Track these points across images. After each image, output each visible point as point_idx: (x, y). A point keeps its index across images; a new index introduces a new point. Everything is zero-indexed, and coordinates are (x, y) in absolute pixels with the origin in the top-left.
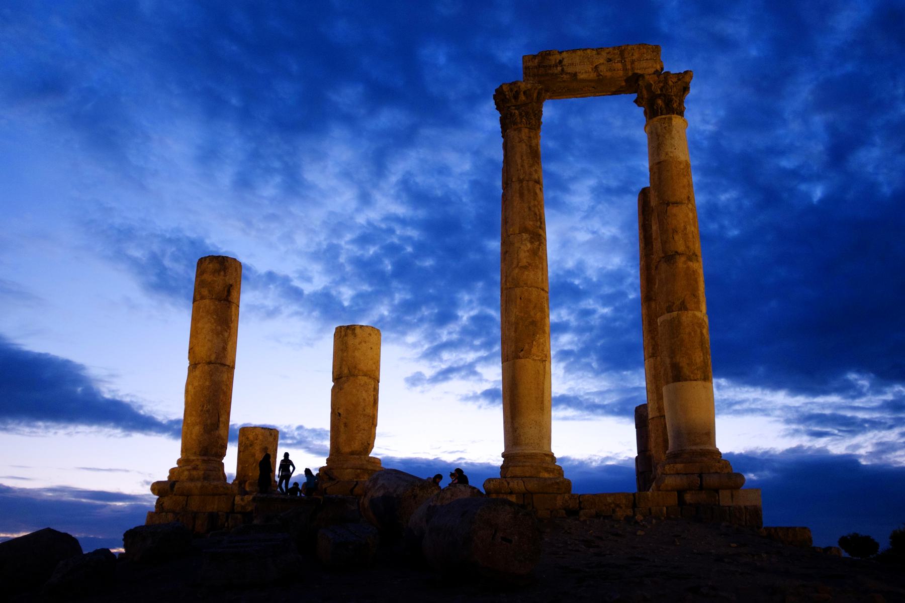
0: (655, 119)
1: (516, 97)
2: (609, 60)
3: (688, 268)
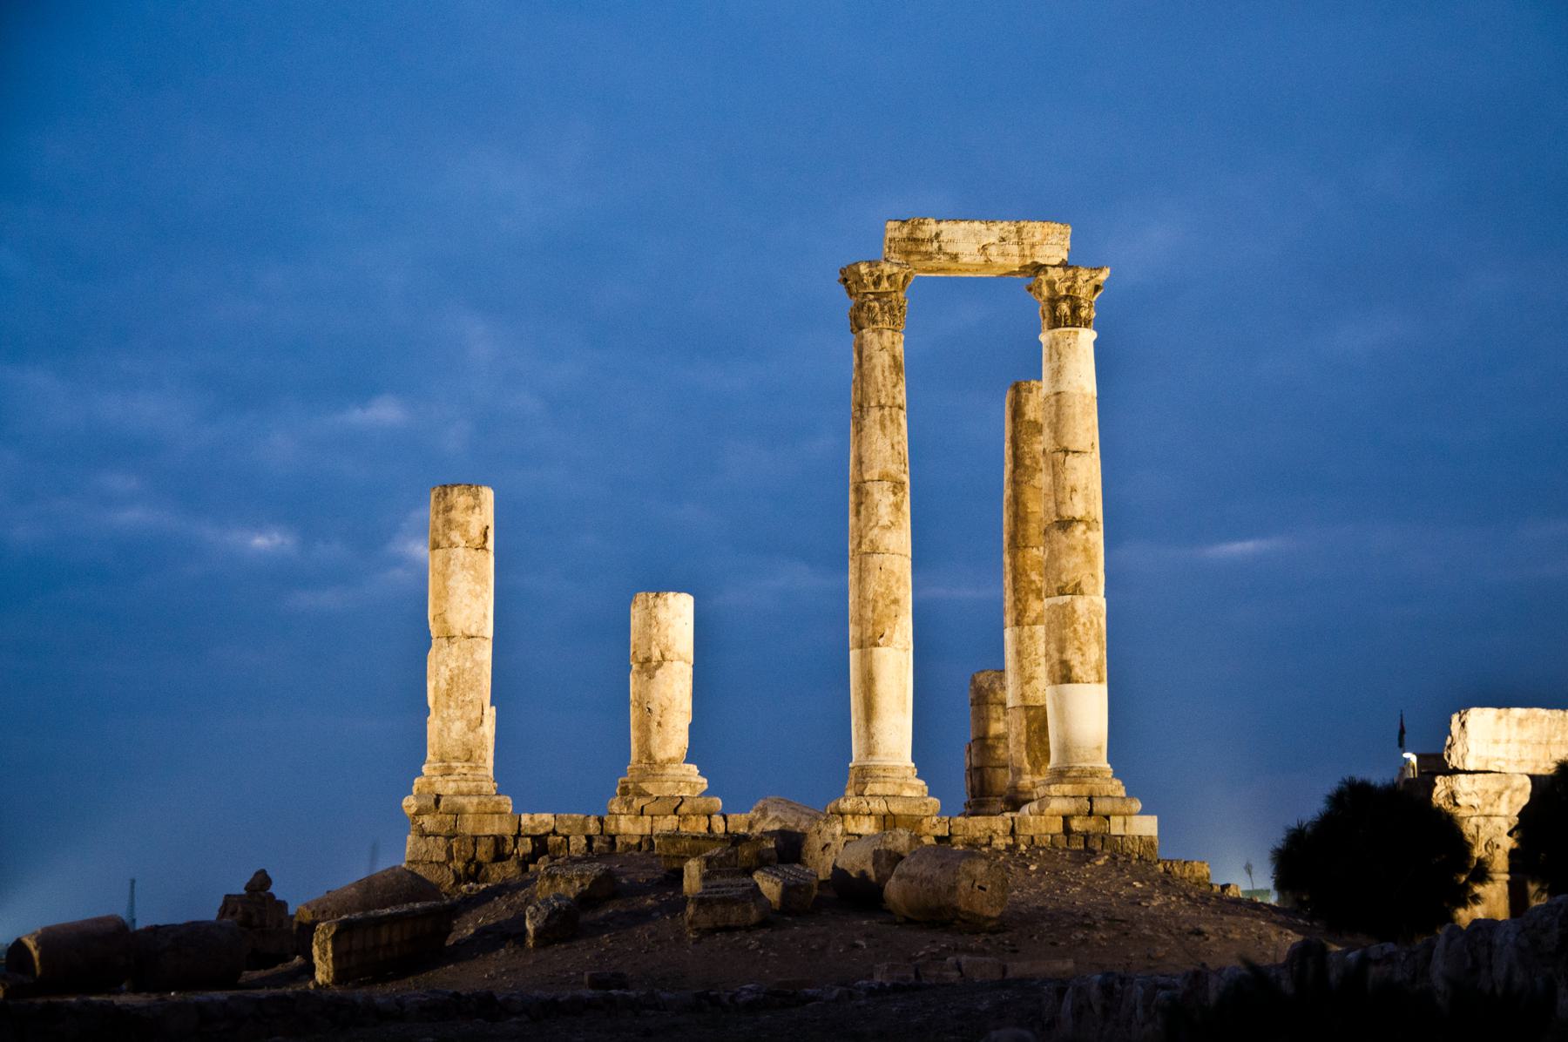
0: (1057, 331)
1: (877, 283)
2: (1003, 240)
3: (1087, 540)
